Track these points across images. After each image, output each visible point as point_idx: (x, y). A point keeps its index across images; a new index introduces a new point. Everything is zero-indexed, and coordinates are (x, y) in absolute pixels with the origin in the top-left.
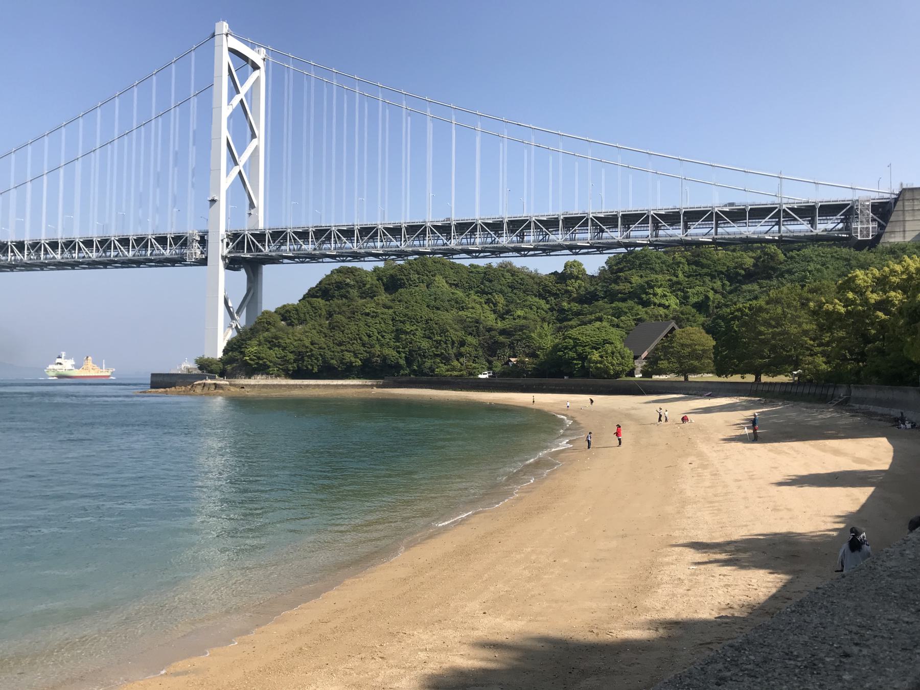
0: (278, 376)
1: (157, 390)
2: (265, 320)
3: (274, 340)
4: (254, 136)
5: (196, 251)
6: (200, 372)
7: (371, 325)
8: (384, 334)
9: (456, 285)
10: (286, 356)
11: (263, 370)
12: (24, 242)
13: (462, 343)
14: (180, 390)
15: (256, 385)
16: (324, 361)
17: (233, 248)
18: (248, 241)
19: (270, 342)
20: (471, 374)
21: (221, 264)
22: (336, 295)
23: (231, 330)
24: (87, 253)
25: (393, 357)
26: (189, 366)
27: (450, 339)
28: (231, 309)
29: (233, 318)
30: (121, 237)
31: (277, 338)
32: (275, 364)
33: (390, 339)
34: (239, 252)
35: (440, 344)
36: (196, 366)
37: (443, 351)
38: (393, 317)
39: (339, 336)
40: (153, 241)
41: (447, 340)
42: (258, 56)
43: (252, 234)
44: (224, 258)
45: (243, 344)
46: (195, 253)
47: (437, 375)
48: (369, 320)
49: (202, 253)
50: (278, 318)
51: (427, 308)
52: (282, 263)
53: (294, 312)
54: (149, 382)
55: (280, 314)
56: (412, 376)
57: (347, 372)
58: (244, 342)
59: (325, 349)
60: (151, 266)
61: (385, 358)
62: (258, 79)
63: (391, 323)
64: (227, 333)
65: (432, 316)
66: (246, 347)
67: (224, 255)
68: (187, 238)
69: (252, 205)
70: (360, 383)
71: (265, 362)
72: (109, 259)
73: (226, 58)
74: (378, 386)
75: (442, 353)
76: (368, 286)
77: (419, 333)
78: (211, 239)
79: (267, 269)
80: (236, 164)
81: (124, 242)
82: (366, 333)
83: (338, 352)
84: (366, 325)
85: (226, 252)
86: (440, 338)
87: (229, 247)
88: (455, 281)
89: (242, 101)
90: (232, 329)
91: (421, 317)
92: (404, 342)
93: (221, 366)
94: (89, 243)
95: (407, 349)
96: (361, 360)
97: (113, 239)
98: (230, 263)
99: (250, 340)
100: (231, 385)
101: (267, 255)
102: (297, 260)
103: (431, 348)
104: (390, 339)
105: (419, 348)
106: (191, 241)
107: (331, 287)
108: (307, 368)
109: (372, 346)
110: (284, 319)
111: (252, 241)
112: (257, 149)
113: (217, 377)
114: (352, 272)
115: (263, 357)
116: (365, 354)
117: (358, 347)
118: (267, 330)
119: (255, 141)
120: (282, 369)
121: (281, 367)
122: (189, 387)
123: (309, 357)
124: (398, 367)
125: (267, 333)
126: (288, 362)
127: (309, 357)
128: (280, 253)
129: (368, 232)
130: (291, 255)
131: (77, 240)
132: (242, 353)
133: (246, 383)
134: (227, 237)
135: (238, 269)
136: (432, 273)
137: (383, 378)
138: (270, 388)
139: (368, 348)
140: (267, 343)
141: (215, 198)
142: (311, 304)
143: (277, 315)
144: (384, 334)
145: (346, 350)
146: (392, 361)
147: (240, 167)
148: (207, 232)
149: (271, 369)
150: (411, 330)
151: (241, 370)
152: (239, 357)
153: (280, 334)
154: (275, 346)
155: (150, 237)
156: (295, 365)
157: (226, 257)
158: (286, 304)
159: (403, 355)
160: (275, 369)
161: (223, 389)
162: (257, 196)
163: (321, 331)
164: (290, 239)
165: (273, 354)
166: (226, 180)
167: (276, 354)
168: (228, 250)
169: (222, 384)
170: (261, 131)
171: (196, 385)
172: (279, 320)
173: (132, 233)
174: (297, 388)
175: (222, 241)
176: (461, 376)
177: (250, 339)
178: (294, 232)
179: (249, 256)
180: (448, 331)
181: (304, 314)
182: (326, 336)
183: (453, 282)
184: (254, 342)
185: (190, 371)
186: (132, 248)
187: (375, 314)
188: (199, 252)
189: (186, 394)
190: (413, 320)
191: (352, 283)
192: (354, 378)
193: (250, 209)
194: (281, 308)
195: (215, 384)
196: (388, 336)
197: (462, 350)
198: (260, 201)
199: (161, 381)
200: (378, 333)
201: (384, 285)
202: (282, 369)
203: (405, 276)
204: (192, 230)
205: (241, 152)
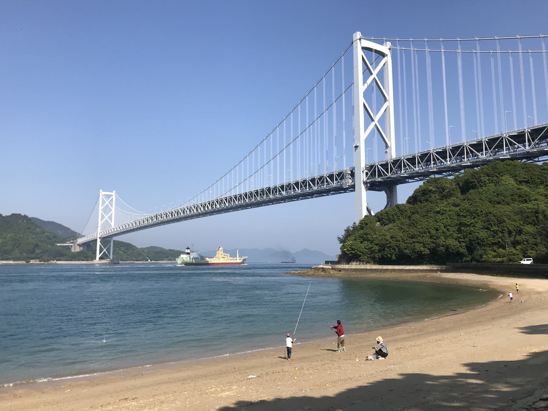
0: (368, 262)
4: (386, 100)
7: (438, 220)
8: (449, 227)
9: (527, 182)
10: (372, 248)
13: (520, 232)
15: (349, 269)
16: (400, 251)
18: (379, 170)
20: (510, 260)
21: (363, 187)
22: (422, 200)
25: (454, 246)
27: (506, 229)
33: (454, 232)
35: (497, 233)
37: (499, 240)
38: (458, 213)
39: (413, 231)
41: (503, 230)
42: (384, 48)
44: (365, 183)
46: (348, 182)
47: (484, 261)
48: (439, 217)
51: (489, 203)
53: (385, 215)
56: (474, 263)
57: (419, 259)
59: (400, 241)
61: (447, 248)
63: (456, 217)
65: (491, 209)
69: (387, 146)
70: (428, 268)
71: (356, 252)
73: (360, 54)
74: (442, 271)
75: (499, 242)
76: (447, 191)
77: (479, 225)
80: (373, 120)
82: (435, 228)
83: (411, 244)
84: (435, 221)
85: (365, 179)
86: (496, 228)
88: (525, 178)
91: (482, 212)
92: (464, 234)
95: (467, 239)
96: (428, 249)
98: (371, 186)
100: (332, 269)
102: (417, 178)
103: (489, 237)
104: (454, 232)
105: (477, 238)
107: (419, 194)
108: (387, 256)
109: (438, 238)
110: (379, 221)
114: (435, 181)
115: (354, 248)
116: (432, 245)
117: (427, 240)
119: (387, 104)
120: (370, 257)
123: (389, 247)
124: (459, 255)
126: (373, 252)
127: (389, 247)
129: (457, 151)
133: (342, 267)
134: (366, 169)
136: (502, 174)
137: (445, 264)
138: (359, 271)
139: (434, 239)
141: (358, 145)
142: (399, 208)
144: (449, 227)
145: (418, 242)
146: (454, 250)
149: (361, 257)
150: (472, 223)
151: (344, 258)
154: (365, 240)
156: (380, 254)
159: (464, 244)
161: (325, 272)
163: (401, 228)
167: (365, 246)
170: (390, 96)
174: (378, 271)
176: (502, 262)
179: (380, 180)
180: (505, 222)
181: (393, 215)
182: (404, 232)
183: (522, 180)
187: (444, 212)
188: (350, 181)
190: (474, 214)
191: (434, 189)
192: (426, 264)
193: (386, 149)
196: (452, 229)
197: (518, 238)
198: (392, 143)
200: (445, 227)
201: (460, 187)
203: (476, 179)
204: (346, 169)
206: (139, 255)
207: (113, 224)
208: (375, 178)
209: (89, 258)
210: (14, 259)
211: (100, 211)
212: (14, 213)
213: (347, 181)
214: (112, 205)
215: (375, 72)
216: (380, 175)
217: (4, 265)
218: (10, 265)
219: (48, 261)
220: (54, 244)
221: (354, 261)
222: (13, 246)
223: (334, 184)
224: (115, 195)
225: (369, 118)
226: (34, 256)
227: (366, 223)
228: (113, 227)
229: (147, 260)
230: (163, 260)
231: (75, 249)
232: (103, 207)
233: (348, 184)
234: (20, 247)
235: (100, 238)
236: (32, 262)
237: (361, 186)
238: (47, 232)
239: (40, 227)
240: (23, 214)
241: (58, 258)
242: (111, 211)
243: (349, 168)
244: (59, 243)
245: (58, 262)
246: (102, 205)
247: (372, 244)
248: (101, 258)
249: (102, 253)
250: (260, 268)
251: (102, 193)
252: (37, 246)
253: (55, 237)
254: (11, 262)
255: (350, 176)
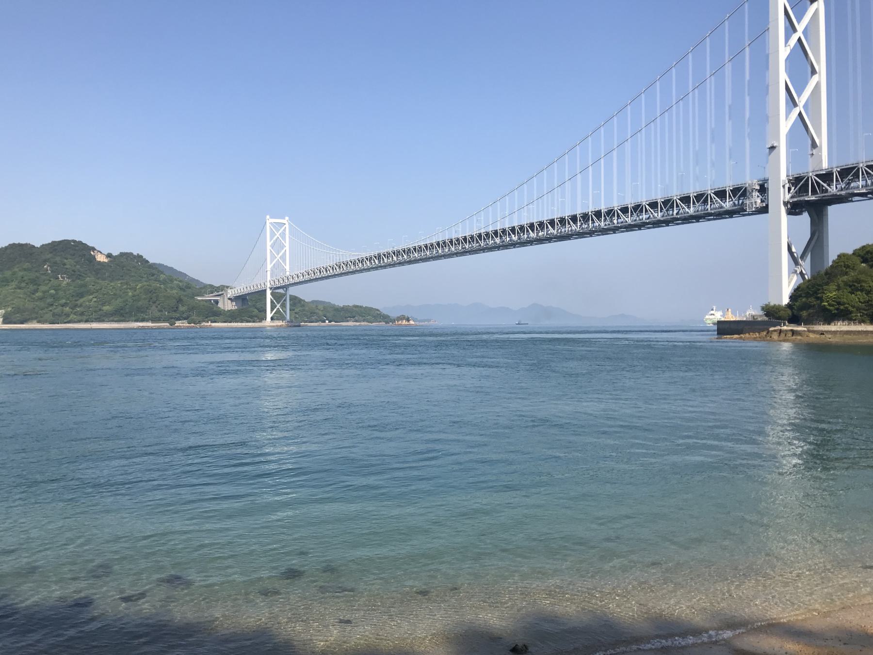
0: (862, 321)
1: (733, 336)
2: (842, 264)
3: (855, 284)
4: (814, 72)
5: (756, 200)
6: (766, 318)
11: (844, 316)
12: (601, 210)
14: (755, 336)
15: (837, 331)
17: (796, 192)
19: (850, 286)
21: (783, 210)
23: (795, 276)
24: (652, 213)
26: (754, 313)
28: (795, 255)
29: (796, 263)
30: (682, 196)
31: (859, 281)
32: (859, 309)
34: (803, 196)
36: (761, 313)
40: (712, 195)
43: (817, 176)
44: (785, 204)
45: (819, 290)
46: (756, 202)
49: (762, 201)
50: (857, 260)
52: (852, 201)
54: (716, 328)
55: (859, 256)
58: (820, 288)
60: (709, 220)
62: (816, 13)
64: (792, 279)
66: (824, 293)
67: (786, 200)
68: (746, 188)
69: (814, 145)
71: (847, 308)
72: (671, 217)
78: (771, 186)
79: (833, 210)
80: (795, 105)
81: (686, 200)
87: (791, 191)
89: (799, 40)
90: (797, 274)
93: (789, 312)
94: (654, 205)
97: (675, 198)
98: (792, 208)
99: (826, 285)
100: (809, 331)
101: (836, 195)
106: (751, 191)
110: (865, 260)
111: (817, 182)
112: (818, 85)
113: (787, 324)
115: (844, 302)
118: (846, 274)
119: (815, 78)
120: (866, 314)
121: (865, 312)
122: (765, 333)
125: (846, 276)
128: (850, 191)
130: (864, 191)
131: (644, 204)
132: (821, 299)
134: (788, 182)
135: (800, 213)
140: (848, 288)
141: (775, 145)
143: (856, 258)
147: (800, 108)
148: (766, 181)
152: (815, 303)
153: (862, 277)
154: (857, 290)
155: (709, 192)
157: (788, 202)
158: (865, 244)
160: (859, 315)
162: (819, 136)
164: (863, 174)
165: (856, 299)
166: (786, 123)
167: (859, 298)
168: (790, 195)
169: (800, 331)
170: (822, 67)
171: (772, 331)
172: (858, 262)
173: (692, 190)
175: (784, 186)
177: (827, 284)
178: (867, 166)
179: (814, 198)
184: (833, 286)
185: (755, 318)
186: (693, 204)
188: (759, 201)
189: (763, 339)
194: (860, 249)
195: (792, 330)
198: (823, 141)
199: (724, 328)
202: (866, 314)
204: (750, 180)
205: (800, 92)
206: (313, 313)
207: (287, 268)
208: (806, 195)
209: (256, 318)
210: (153, 321)
211: (269, 248)
212: (123, 251)
213: (753, 201)
214: (284, 239)
215: (800, 27)
216: (814, 192)
217: (140, 329)
218: (148, 328)
219: (200, 322)
220: (193, 298)
221: (838, 320)
222: (149, 301)
223: (728, 205)
224: (289, 224)
225: (792, 102)
226: (178, 315)
227: (847, 265)
228: (288, 273)
229: (324, 322)
230: (348, 321)
231: (224, 304)
232: (272, 241)
233: (754, 206)
234: (158, 302)
235: (271, 289)
236: (178, 324)
237: (780, 207)
238: (176, 280)
239: (162, 273)
240: (135, 253)
241: (212, 318)
242: (283, 249)
243: (756, 181)
244: (198, 296)
245: (214, 324)
246: (271, 239)
247: (870, 295)
248: (272, 319)
249: (275, 310)
250: (656, 331)
251: (270, 221)
252: (180, 300)
253: (188, 287)
254: (150, 324)
255: (757, 194)
